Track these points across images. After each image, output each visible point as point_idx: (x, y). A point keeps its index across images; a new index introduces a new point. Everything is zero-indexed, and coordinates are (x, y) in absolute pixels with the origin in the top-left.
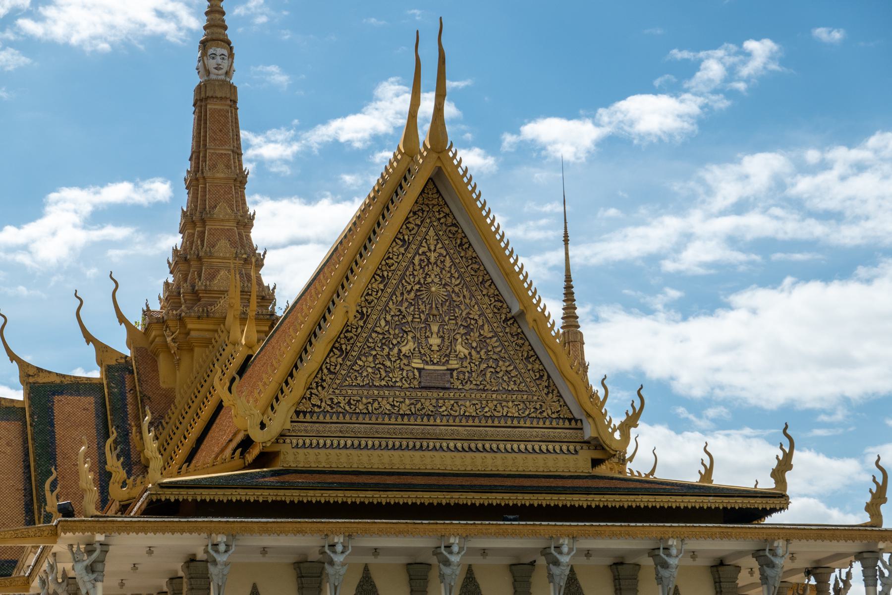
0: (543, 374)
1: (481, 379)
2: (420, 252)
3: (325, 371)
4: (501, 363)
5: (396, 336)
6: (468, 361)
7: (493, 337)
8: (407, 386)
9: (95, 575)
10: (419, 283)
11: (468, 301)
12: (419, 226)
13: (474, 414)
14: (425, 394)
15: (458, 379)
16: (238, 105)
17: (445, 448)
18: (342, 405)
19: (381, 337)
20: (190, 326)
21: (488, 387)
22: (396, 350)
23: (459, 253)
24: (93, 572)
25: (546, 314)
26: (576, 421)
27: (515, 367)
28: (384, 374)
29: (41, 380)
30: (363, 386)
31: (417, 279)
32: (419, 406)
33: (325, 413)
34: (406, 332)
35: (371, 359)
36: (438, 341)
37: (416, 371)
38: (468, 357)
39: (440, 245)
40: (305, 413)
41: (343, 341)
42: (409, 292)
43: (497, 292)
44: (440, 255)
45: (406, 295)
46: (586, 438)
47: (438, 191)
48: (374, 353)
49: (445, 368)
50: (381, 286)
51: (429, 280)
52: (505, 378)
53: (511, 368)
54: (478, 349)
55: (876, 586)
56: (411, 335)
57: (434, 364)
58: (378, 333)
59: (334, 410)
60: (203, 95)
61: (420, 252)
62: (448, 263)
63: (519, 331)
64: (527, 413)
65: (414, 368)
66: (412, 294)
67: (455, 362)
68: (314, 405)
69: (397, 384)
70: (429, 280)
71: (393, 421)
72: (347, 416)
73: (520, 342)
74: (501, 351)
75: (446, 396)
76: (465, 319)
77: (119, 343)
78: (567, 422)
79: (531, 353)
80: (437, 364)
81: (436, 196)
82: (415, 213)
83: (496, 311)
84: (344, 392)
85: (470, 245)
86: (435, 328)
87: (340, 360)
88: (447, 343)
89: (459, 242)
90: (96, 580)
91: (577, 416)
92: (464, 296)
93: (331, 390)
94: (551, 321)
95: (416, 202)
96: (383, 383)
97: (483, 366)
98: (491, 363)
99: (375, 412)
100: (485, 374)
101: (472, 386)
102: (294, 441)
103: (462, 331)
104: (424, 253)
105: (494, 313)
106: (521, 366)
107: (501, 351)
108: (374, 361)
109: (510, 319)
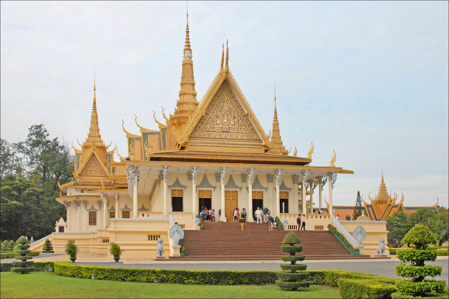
0: (253, 129)
2: (222, 98)
3: (198, 127)
4: (242, 126)
5: (215, 119)
8: (218, 131)
9: (135, 174)
10: (222, 106)
11: (234, 111)
12: (222, 92)
13: (235, 138)
14: (223, 133)
16: (193, 66)
17: (228, 147)
19: (212, 119)
20: (180, 119)
21: (239, 132)
23: (232, 99)
24: (134, 173)
25: (254, 114)
26: (261, 140)
28: (212, 128)
29: (144, 132)
31: (221, 105)
32: (221, 136)
35: (209, 124)
39: (227, 97)
40: (192, 137)
41: (202, 120)
42: (219, 108)
43: (242, 109)
44: (227, 99)
45: (218, 109)
46: (263, 145)
47: (227, 83)
48: (210, 123)
49: (228, 127)
50: (212, 107)
51: (224, 105)
52: (243, 130)
55: (331, 181)
56: (219, 119)
60: (184, 63)
61: (222, 98)
62: (229, 102)
63: (247, 118)
64: (249, 138)
66: (220, 109)
68: (195, 136)
70: (224, 105)
75: (228, 134)
77: (164, 122)
78: (259, 141)
79: (250, 124)
80: (226, 126)
81: (227, 84)
82: (221, 89)
85: (235, 97)
86: (226, 117)
87: (201, 125)
88: (229, 121)
89: (232, 96)
90: (135, 175)
91: (262, 139)
92: (233, 110)
93: (199, 132)
94: (255, 116)
95: (221, 86)
96: (212, 130)
97: (238, 127)
98: (240, 126)
100: (238, 129)
101: (235, 132)
103: (233, 118)
104: (223, 99)
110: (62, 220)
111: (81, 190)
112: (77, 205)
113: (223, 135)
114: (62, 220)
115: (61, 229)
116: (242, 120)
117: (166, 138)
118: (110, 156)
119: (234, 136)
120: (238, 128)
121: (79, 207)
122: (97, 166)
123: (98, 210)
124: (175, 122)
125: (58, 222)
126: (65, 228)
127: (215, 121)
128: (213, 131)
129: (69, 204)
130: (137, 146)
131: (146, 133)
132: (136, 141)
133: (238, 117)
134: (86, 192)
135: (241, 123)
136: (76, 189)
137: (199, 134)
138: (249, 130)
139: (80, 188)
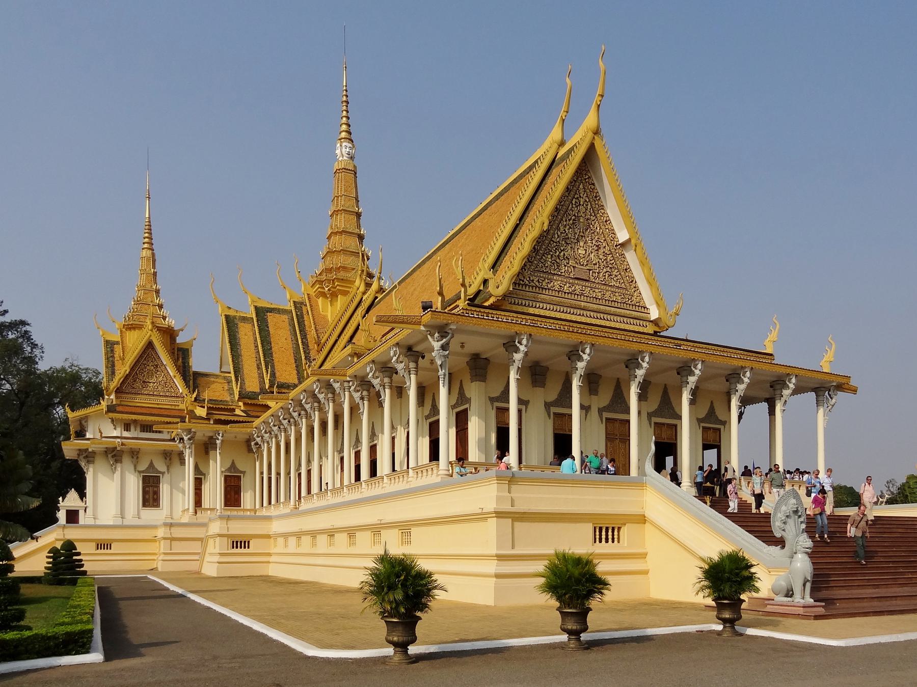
1: (604, 278)
4: (613, 270)
6: (598, 266)
7: (610, 254)
8: (567, 275)
14: (576, 282)
15: (593, 276)
18: (534, 282)
22: (562, 254)
27: (620, 274)
28: (556, 267)
30: (545, 272)
33: (526, 285)
34: (568, 244)
35: (549, 256)
36: (585, 251)
37: (572, 267)
38: (598, 264)
48: (551, 253)
53: (619, 273)
54: (603, 260)
57: (581, 265)
58: (554, 242)
59: (531, 284)
65: (571, 266)
67: (591, 266)
68: (520, 280)
69: (563, 274)
71: (560, 295)
72: (537, 289)
73: (623, 259)
74: (613, 263)
76: (597, 241)
80: (582, 265)
83: (612, 239)
84: (536, 274)
88: (587, 254)
96: (555, 272)
99: (551, 288)
102: (510, 300)
105: (611, 240)
106: (623, 273)
107: (613, 263)
108: (551, 258)
109: (619, 245)
110: (73, 495)
111: (125, 424)
112: (116, 461)
113: (577, 286)
114: (73, 495)
115: (73, 517)
116: (612, 256)
117: (306, 323)
118: (183, 354)
119: (597, 291)
120: (606, 273)
121: (119, 465)
122: (158, 373)
123: (163, 473)
124: (327, 289)
125: (63, 501)
126: (81, 513)
127: (562, 251)
128: (558, 275)
129: (90, 456)
130: (245, 335)
131: (262, 307)
132: (242, 324)
133: (605, 247)
134: (135, 431)
135: (611, 262)
136: (113, 421)
137: (529, 277)
138: (626, 282)
139: (122, 419)
